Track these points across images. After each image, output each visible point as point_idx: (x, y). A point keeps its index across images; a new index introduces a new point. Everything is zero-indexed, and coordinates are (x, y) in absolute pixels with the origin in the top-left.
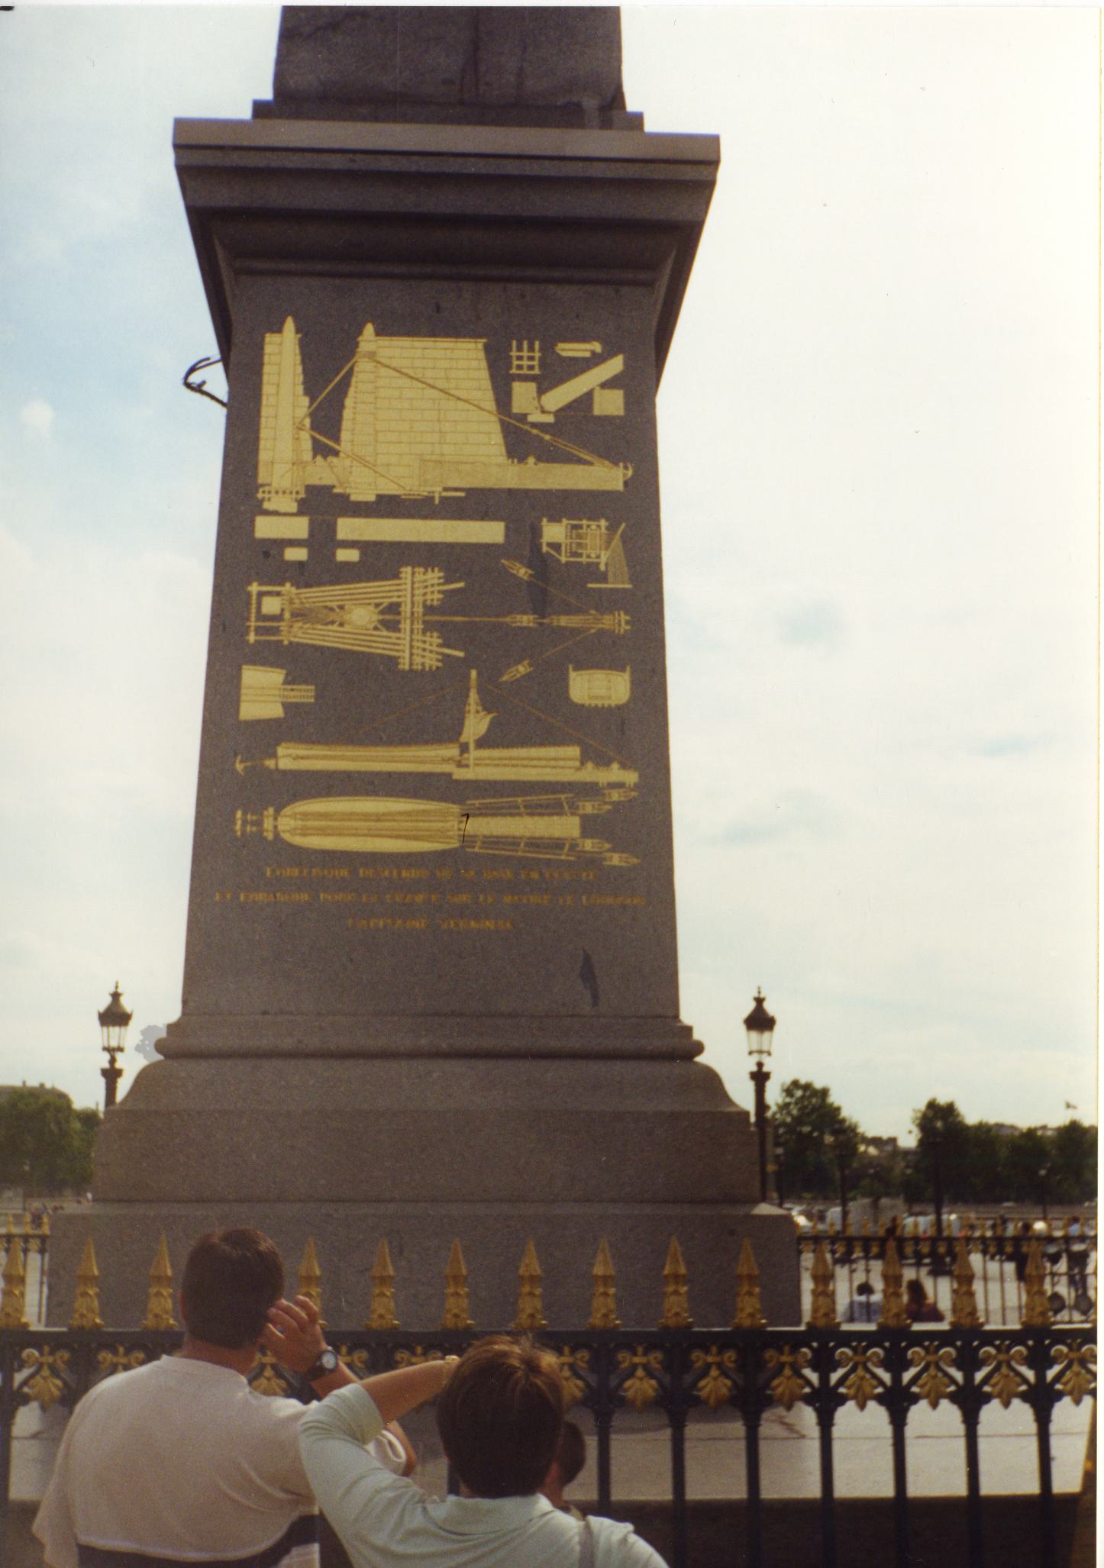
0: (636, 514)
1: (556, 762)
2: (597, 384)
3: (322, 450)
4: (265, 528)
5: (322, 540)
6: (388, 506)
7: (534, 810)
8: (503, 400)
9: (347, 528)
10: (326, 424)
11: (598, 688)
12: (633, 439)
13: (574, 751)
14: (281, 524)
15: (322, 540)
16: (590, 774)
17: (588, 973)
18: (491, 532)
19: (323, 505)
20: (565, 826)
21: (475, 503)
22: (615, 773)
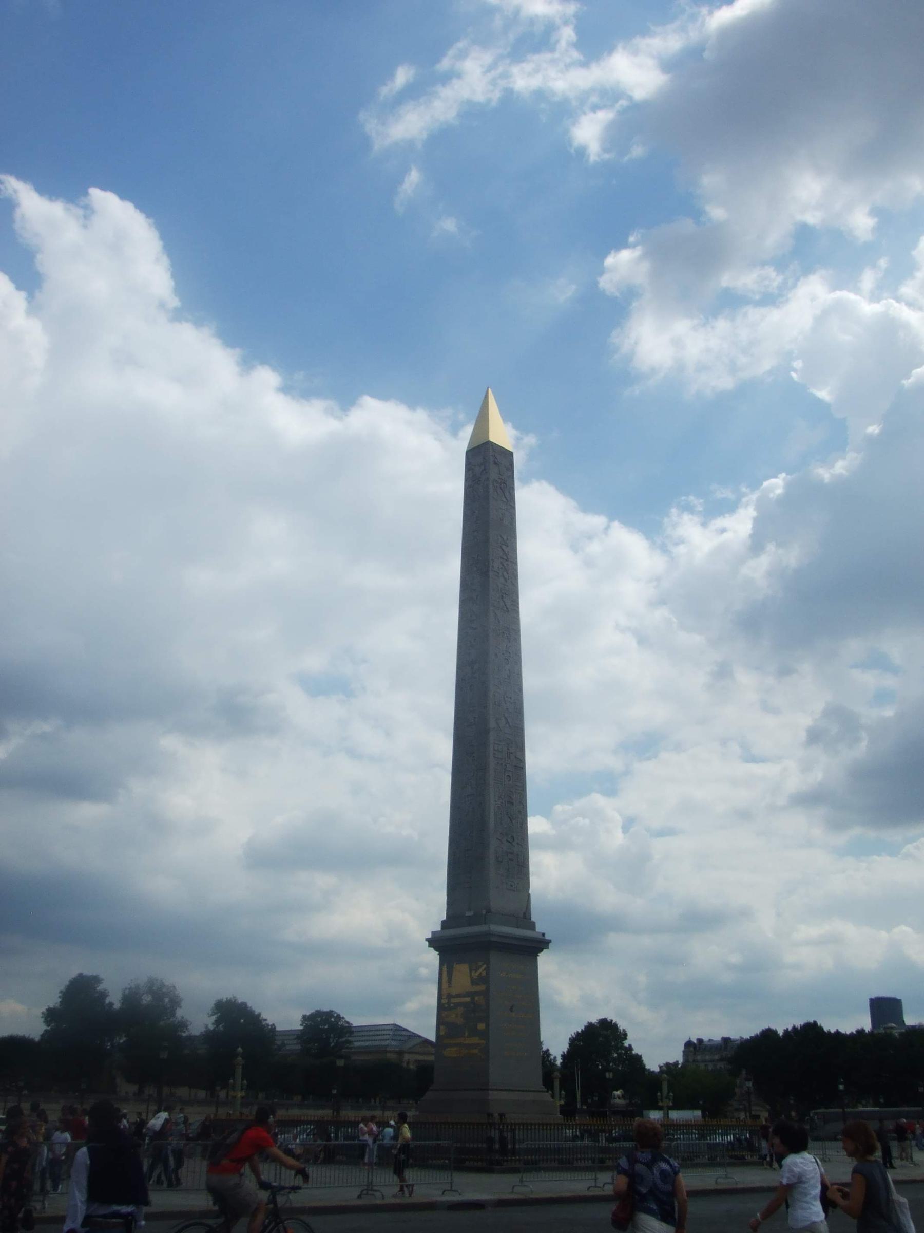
0: (486, 994)
1: (475, 1040)
2: (482, 970)
3: (449, 987)
4: (443, 1001)
9: (454, 1000)
10: (450, 981)
11: (481, 1026)
14: (444, 1001)
15: (449, 1003)
18: (468, 999)
19: (449, 996)
20: (476, 1051)
21: (468, 994)
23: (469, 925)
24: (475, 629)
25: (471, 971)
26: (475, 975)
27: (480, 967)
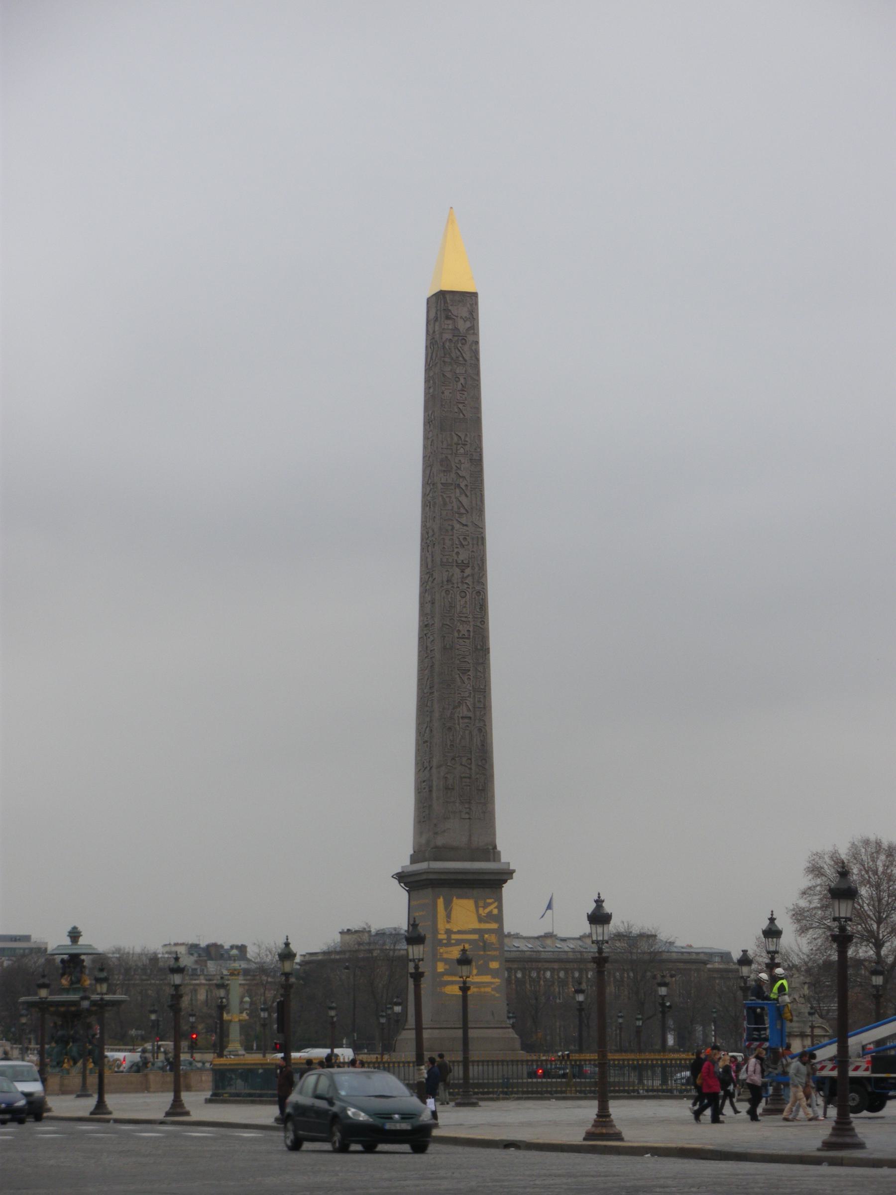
1: (487, 979)
2: (493, 908)
4: (440, 937)
5: (449, 939)
6: (459, 932)
7: (484, 987)
8: (477, 911)
9: (454, 936)
11: (494, 965)
12: (498, 918)
13: (489, 977)
14: (442, 936)
15: (449, 939)
16: (493, 980)
17: (493, 1014)
18: (475, 937)
19: (449, 932)
20: (488, 990)
21: (474, 931)
22: (497, 980)
23: (472, 860)
24: (466, 525)
25: (477, 907)
26: (483, 912)
27: (490, 904)
